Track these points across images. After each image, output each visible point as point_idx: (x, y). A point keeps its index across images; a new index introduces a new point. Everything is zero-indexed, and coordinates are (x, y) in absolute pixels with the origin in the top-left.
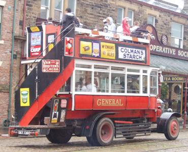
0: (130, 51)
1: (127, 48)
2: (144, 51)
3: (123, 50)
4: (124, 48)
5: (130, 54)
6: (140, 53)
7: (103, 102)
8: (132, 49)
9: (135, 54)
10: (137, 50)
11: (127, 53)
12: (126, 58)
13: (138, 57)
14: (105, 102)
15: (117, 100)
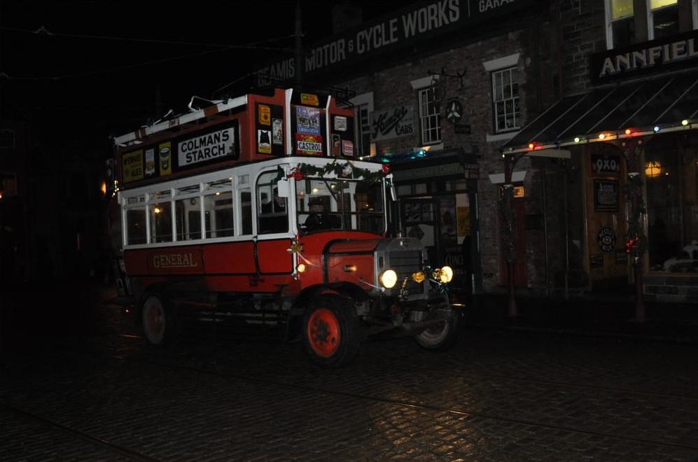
0: (198, 144)
1: (193, 140)
2: (231, 131)
3: (185, 147)
4: (187, 142)
5: (198, 150)
6: (221, 138)
7: (162, 260)
8: (203, 137)
9: (210, 146)
10: (212, 135)
11: (194, 150)
12: (193, 162)
13: (216, 151)
14: (165, 261)
15: (186, 256)
